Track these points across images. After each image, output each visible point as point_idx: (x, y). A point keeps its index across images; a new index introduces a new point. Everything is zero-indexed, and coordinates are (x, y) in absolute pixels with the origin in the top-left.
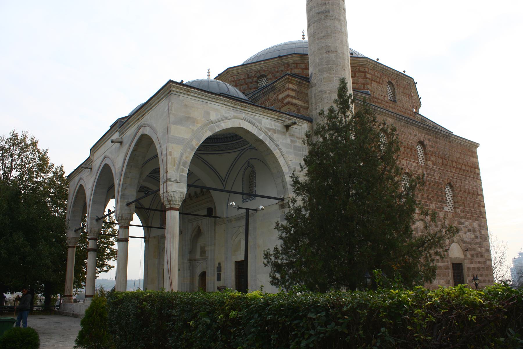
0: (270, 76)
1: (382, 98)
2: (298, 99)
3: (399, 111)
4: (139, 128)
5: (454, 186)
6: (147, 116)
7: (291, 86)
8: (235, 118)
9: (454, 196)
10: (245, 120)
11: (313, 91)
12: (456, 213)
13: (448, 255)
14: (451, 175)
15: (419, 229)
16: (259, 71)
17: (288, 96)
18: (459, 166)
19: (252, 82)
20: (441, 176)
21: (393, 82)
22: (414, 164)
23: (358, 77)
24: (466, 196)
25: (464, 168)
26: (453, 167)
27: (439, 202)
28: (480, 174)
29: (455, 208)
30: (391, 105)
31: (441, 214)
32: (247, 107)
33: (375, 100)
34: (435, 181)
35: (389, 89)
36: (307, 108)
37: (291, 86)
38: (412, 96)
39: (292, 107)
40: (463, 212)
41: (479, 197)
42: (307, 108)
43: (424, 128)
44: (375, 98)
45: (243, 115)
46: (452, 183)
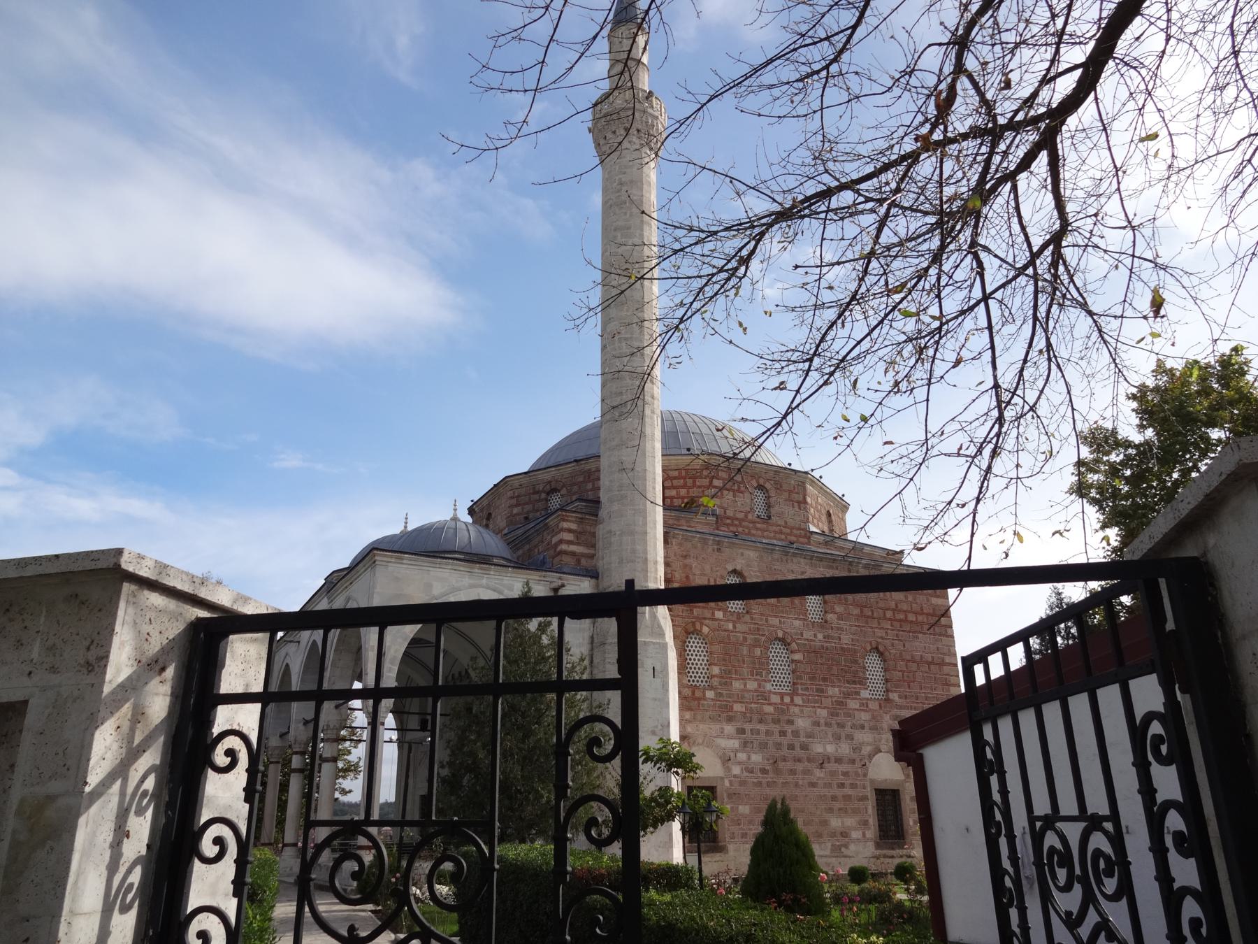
0: (564, 491)
1: (741, 516)
2: (578, 544)
3: (775, 532)
4: (348, 599)
5: (887, 654)
6: (355, 586)
7: (565, 525)
8: (471, 586)
9: (886, 670)
10: (488, 588)
11: (601, 530)
12: (887, 700)
13: (865, 775)
14: (880, 633)
15: (802, 734)
16: (550, 482)
17: (561, 541)
18: (902, 617)
19: (539, 500)
20: (856, 637)
21: (768, 486)
22: (797, 623)
23: (699, 487)
24: (914, 669)
25: (911, 617)
26: (885, 618)
27: (848, 682)
28: (951, 627)
29: (888, 691)
30: (759, 525)
31: (853, 704)
32: (489, 570)
33: (728, 521)
34: (842, 649)
35: (759, 498)
36: (592, 556)
37: (565, 525)
38: (805, 502)
39: (566, 559)
40: (906, 697)
41: (946, 669)
42: (592, 556)
43: (821, 559)
44: (728, 518)
45: (484, 581)
46: (881, 649)
